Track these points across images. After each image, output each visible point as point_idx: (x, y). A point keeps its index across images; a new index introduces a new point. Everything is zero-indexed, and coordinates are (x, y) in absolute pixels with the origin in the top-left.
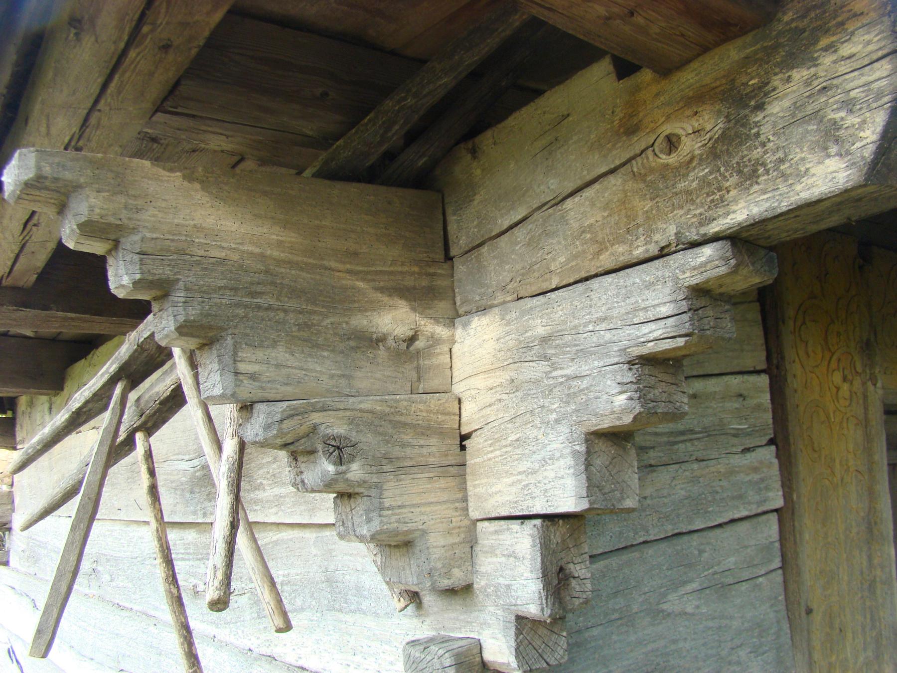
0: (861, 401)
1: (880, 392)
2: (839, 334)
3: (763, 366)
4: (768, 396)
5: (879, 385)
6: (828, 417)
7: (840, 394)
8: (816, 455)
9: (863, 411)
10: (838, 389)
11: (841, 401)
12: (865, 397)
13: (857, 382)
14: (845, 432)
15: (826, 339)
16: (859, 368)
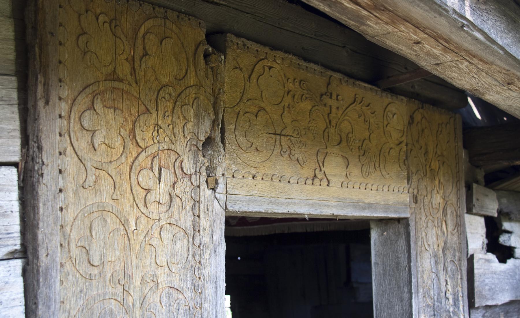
0: (189, 208)
1: (222, 198)
2: (157, 126)
3: (16, 158)
4: (15, 195)
5: (221, 189)
6: (125, 224)
7: (152, 197)
8: (95, 271)
9: (190, 218)
10: (148, 191)
11: (153, 207)
12: (197, 202)
13: (184, 187)
14: (155, 241)
15: (133, 131)
16: (189, 168)
